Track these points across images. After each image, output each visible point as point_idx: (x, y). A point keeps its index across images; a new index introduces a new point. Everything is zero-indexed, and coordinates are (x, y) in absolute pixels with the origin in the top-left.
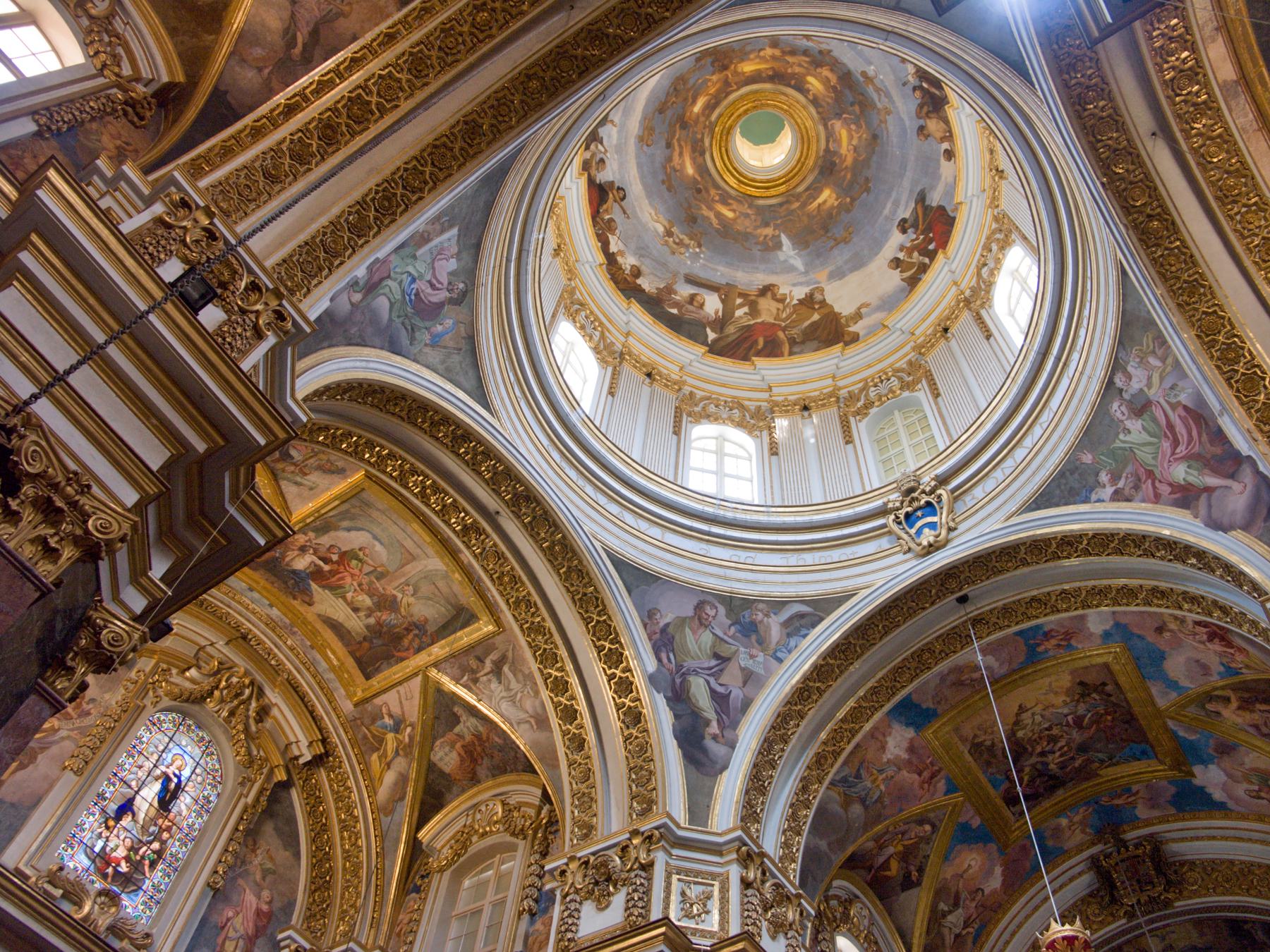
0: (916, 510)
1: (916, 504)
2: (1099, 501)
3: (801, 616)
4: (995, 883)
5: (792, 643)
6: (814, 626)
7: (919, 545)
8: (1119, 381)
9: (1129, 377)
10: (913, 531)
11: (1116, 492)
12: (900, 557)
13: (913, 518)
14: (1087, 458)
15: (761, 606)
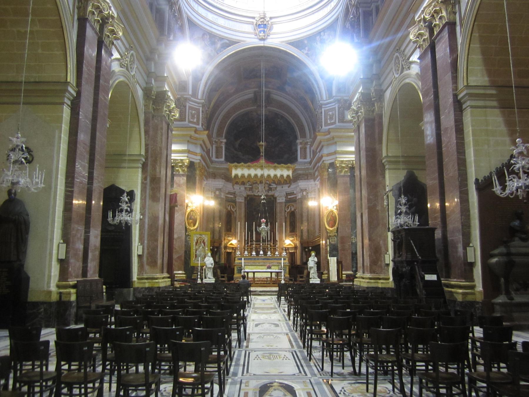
0: (261, 24)
1: (262, 23)
2: (303, 52)
3: (226, 43)
4: (232, 91)
5: (222, 49)
6: (228, 47)
7: (260, 36)
8: (322, 34)
9: (324, 35)
10: (259, 30)
11: (307, 53)
12: (253, 36)
13: (260, 26)
14: (306, 42)
15: (218, 38)
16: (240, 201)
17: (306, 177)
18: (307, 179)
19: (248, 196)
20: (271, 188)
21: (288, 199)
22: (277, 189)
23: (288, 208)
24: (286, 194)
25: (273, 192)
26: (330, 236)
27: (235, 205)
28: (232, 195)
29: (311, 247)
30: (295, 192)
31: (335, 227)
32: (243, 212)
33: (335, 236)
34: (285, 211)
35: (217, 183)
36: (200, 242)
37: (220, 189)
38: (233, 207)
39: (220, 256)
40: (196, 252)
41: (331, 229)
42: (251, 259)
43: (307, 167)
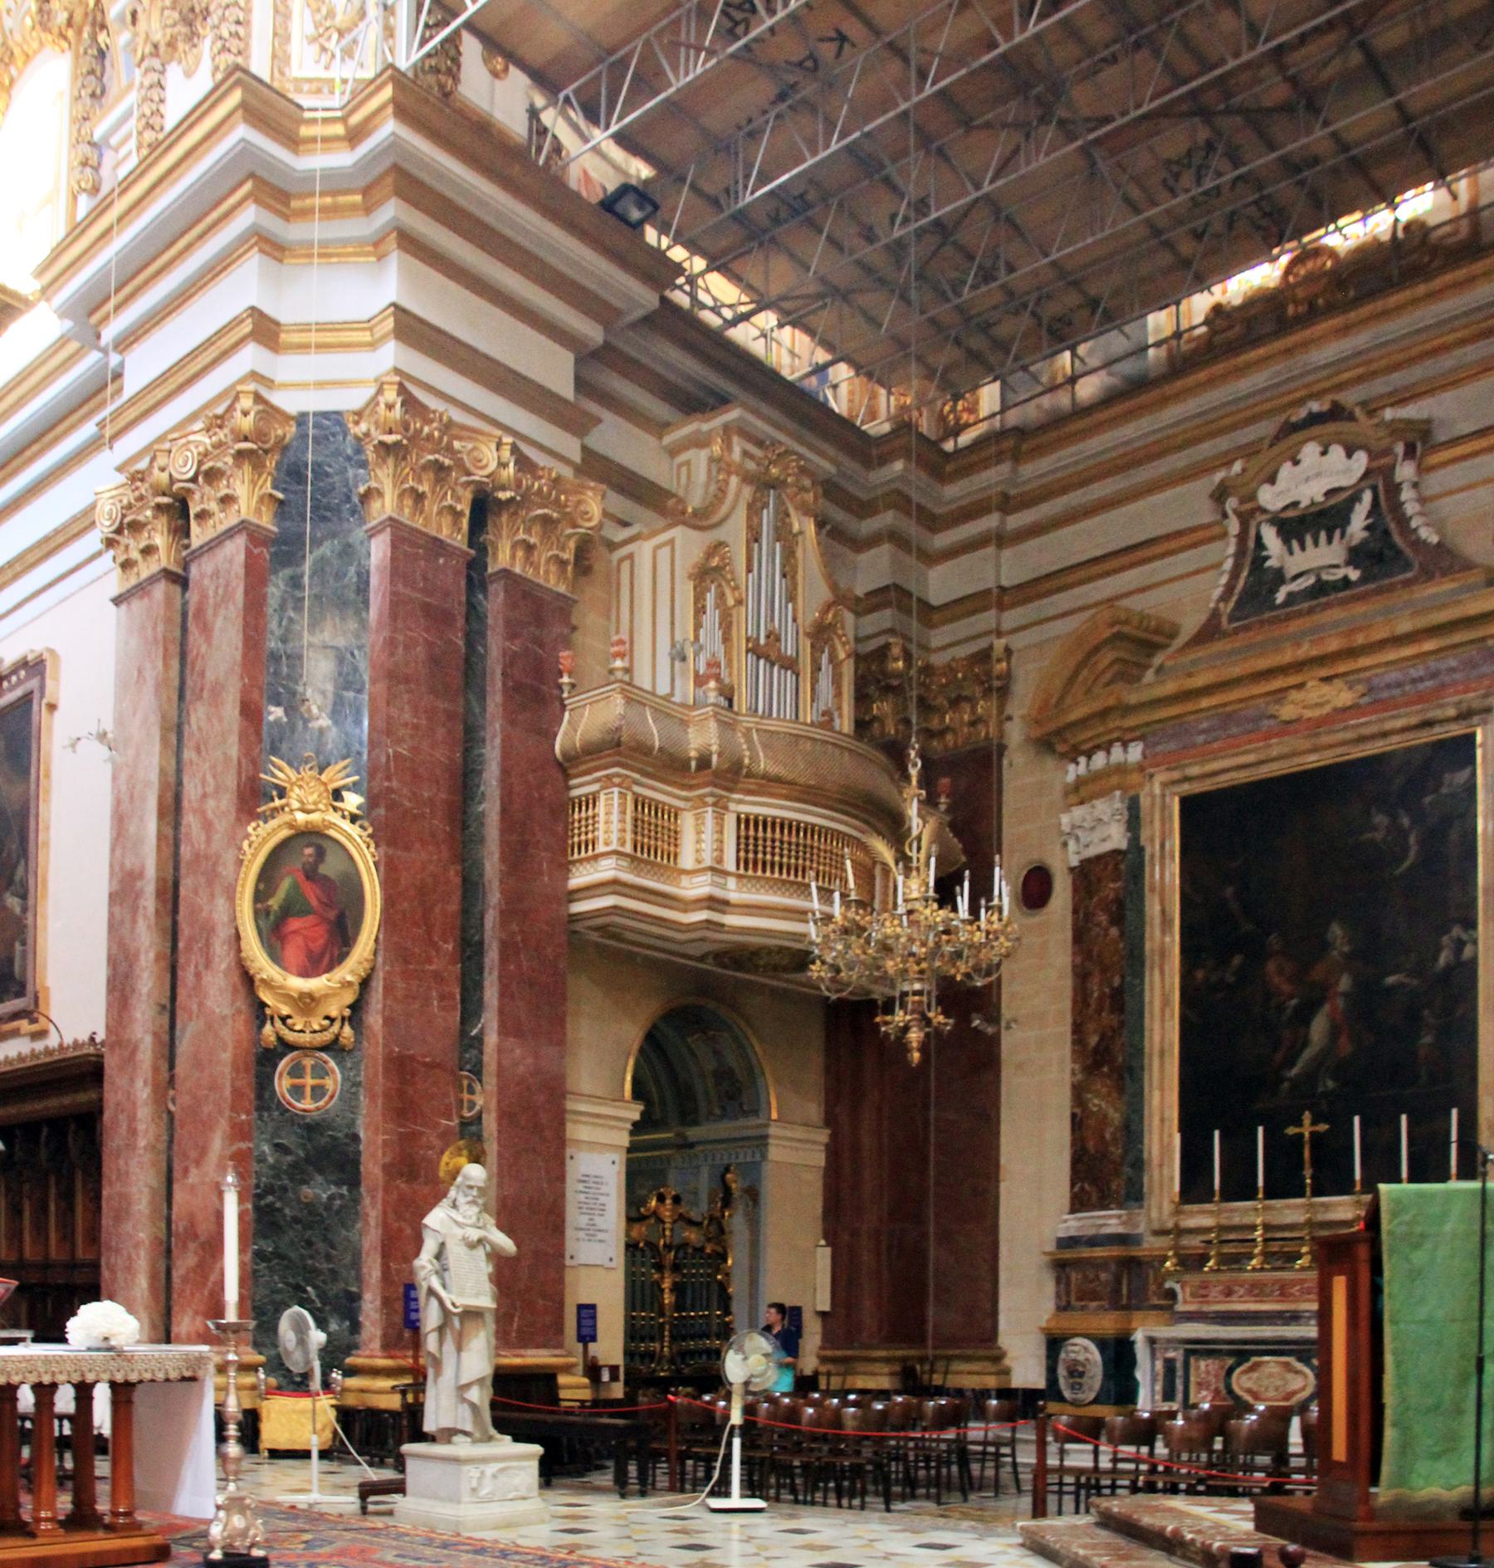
26: (286, 1047)
33: (333, 1047)
41: (297, 983)
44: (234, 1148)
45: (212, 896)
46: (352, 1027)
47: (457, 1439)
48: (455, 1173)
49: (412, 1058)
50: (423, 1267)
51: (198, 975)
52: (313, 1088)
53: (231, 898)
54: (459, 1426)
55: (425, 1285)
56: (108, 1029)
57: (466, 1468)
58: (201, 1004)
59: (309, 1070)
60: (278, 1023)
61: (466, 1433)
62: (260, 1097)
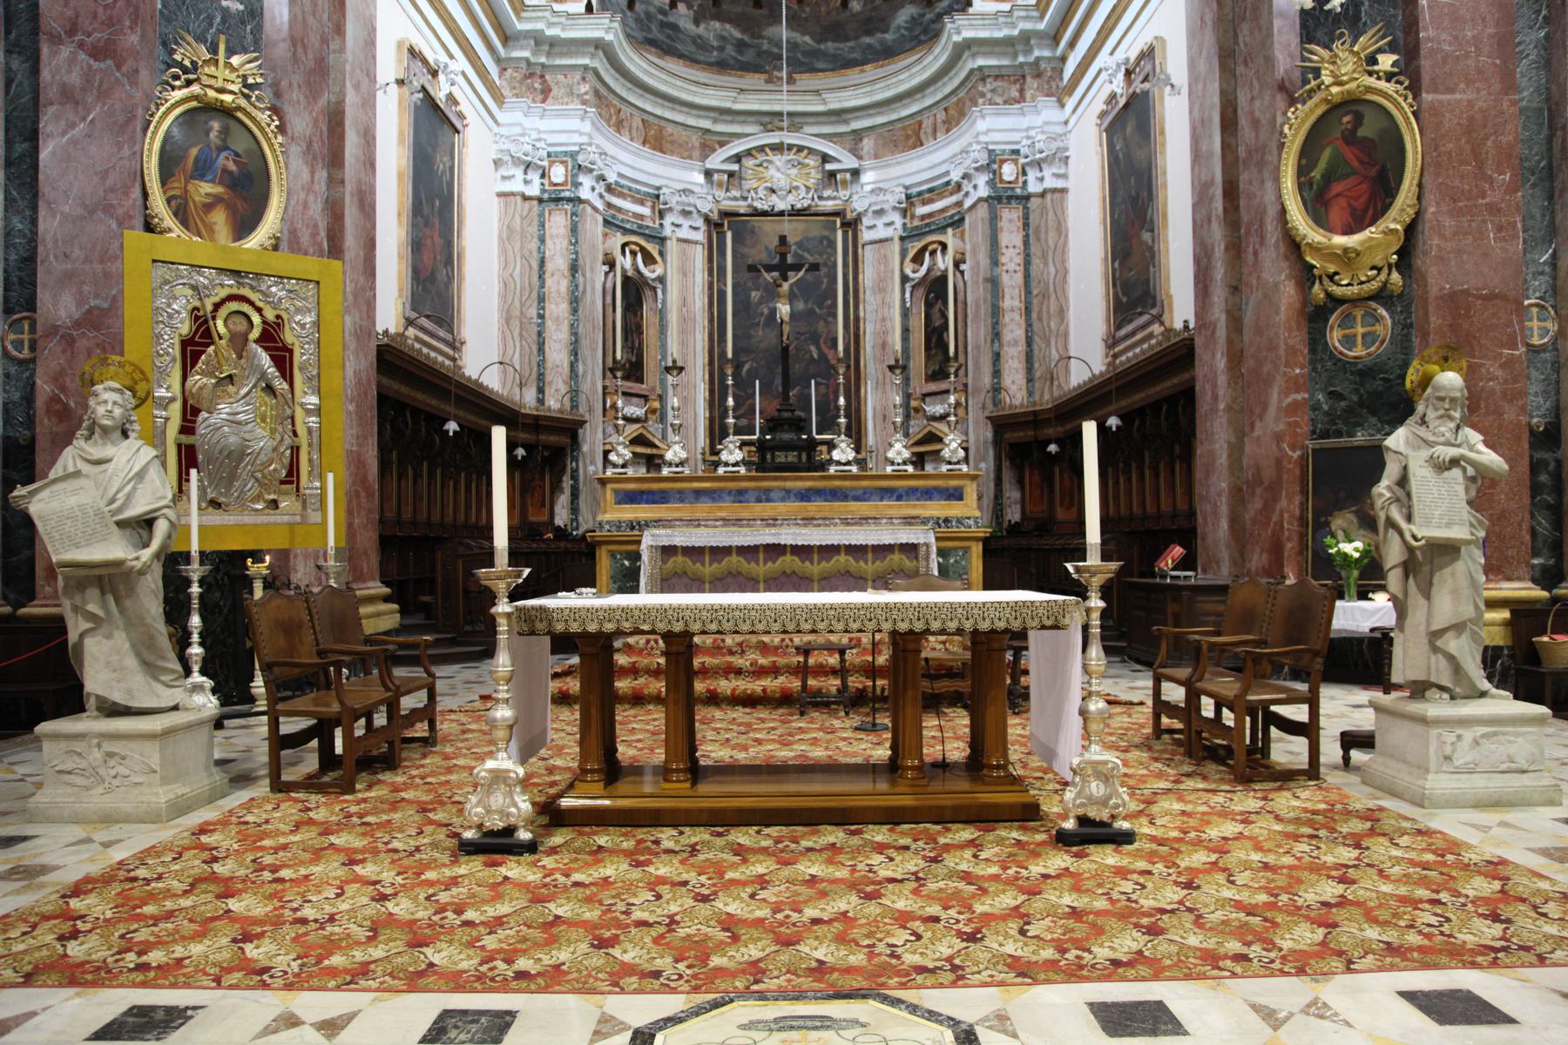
16: (684, 233)
17: (1015, 94)
18: (1022, 99)
19: (726, 214)
20: (832, 175)
21: (916, 223)
22: (867, 177)
23: (918, 259)
24: (908, 197)
25: (843, 194)
26: (1335, 301)
27: (661, 254)
28: (642, 203)
29: (1057, 442)
30: (955, 176)
31: (1393, 222)
32: (698, 289)
33: (1382, 296)
34: (905, 279)
35: (557, 124)
36: (239, 342)
37: (573, 155)
38: (649, 259)
39: (575, 494)
40: (187, 428)
41: (1340, 240)
42: (712, 495)
43: (1028, 26)
44: (1289, 400)
45: (1263, 182)
46: (1400, 272)
47: (1433, 694)
48: (1426, 381)
49: (1466, 292)
50: (1381, 495)
51: (1255, 253)
52: (1364, 336)
53: (1277, 180)
54: (1433, 679)
55: (1382, 515)
56: (1197, 315)
57: (1434, 732)
58: (1258, 278)
59: (1359, 320)
60: (1326, 281)
61: (1442, 688)
62: (1313, 351)
